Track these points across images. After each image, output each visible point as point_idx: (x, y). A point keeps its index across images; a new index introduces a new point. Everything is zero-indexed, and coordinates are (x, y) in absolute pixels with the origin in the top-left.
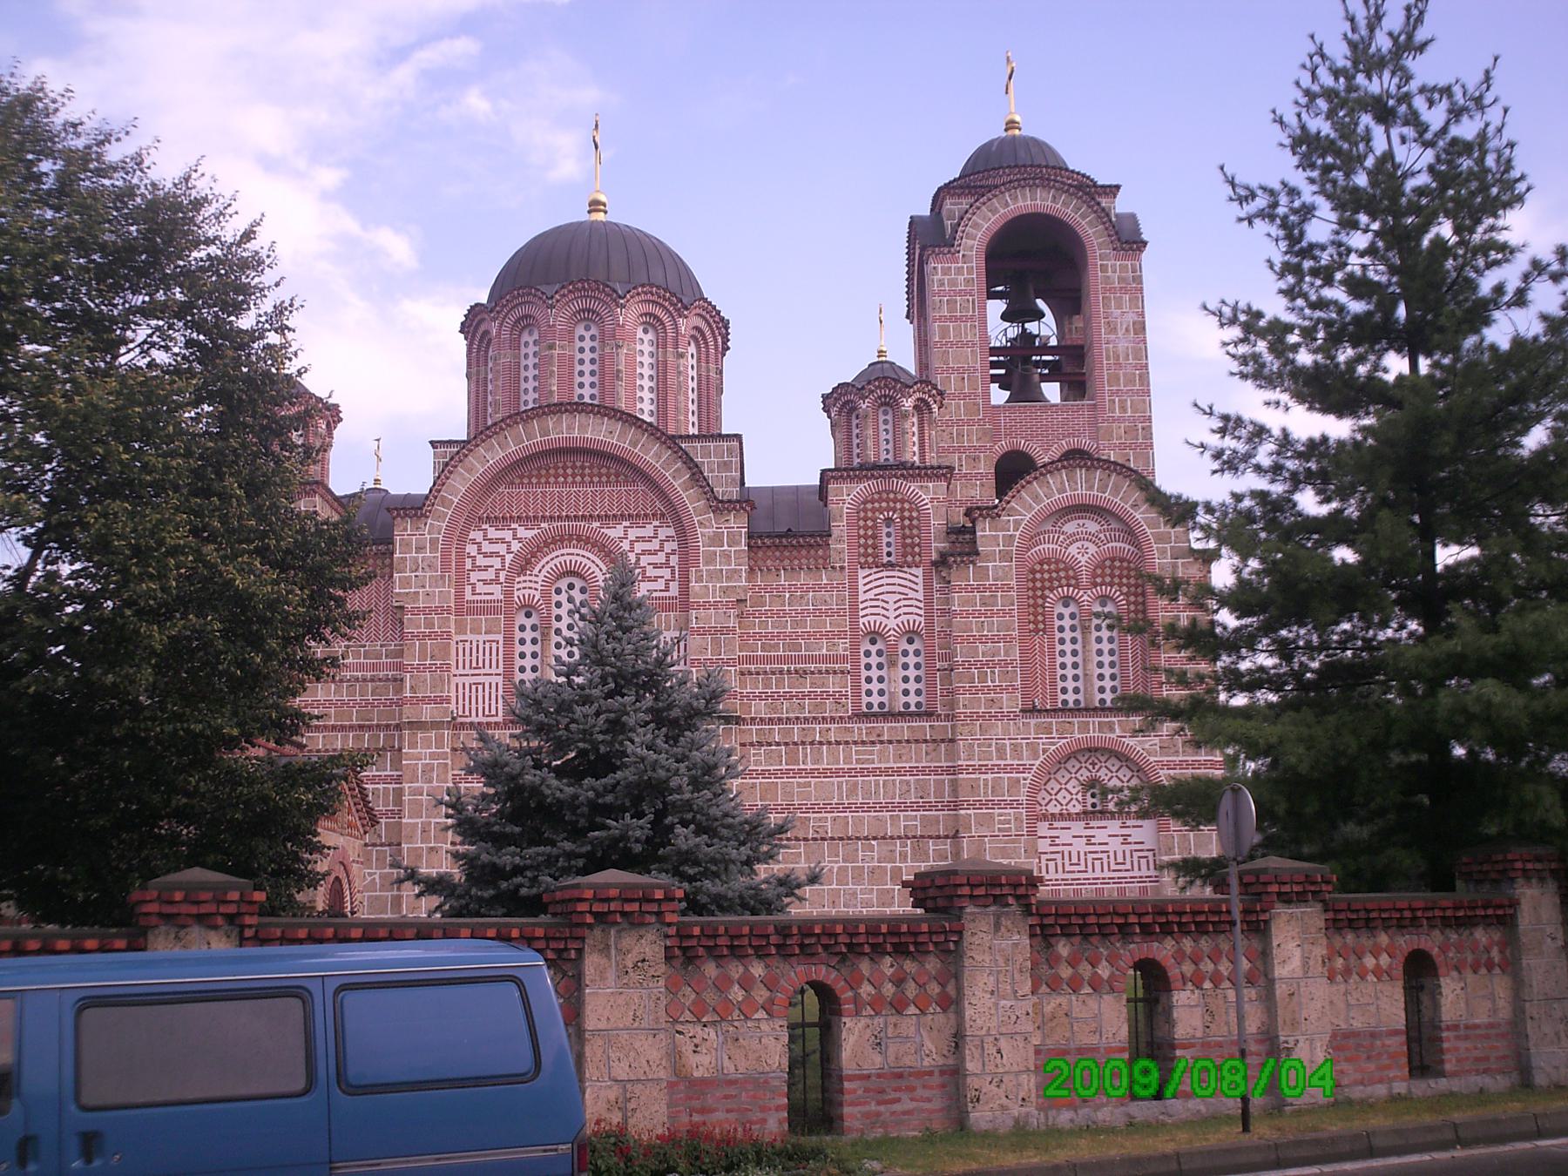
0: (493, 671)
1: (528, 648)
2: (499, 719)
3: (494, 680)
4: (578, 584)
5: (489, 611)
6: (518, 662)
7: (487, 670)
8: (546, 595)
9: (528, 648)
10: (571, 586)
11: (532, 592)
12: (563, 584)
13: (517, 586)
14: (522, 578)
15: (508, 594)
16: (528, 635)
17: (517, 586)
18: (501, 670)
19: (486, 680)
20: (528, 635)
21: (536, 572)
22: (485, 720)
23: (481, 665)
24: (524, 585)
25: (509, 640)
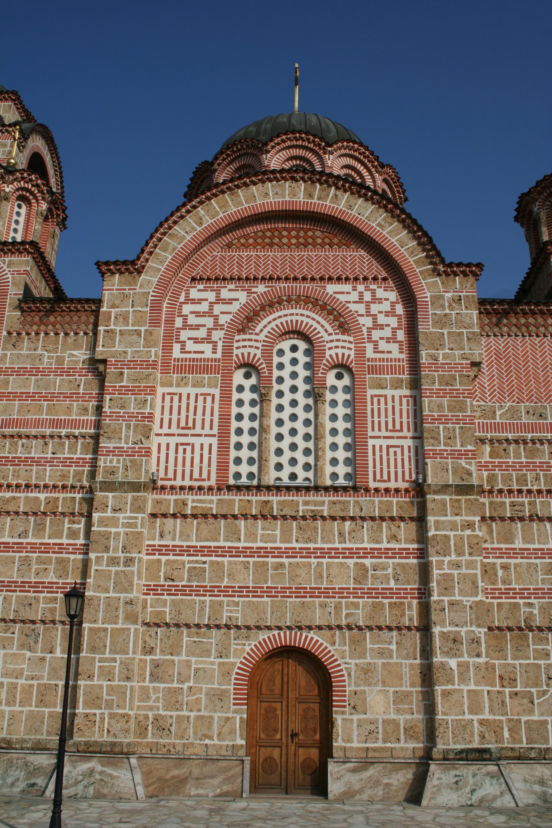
0: (207, 431)
1: (246, 410)
2: (213, 482)
3: (207, 441)
4: (302, 346)
5: (206, 369)
6: (234, 424)
7: (198, 430)
8: (267, 355)
9: (246, 410)
10: (294, 349)
11: (253, 351)
12: (286, 345)
13: (236, 345)
14: (242, 337)
15: (227, 351)
16: (247, 396)
17: (236, 345)
18: (215, 431)
19: (198, 441)
20: (247, 396)
21: (257, 330)
22: (196, 484)
23: (190, 424)
24: (247, 343)
25: (226, 396)
